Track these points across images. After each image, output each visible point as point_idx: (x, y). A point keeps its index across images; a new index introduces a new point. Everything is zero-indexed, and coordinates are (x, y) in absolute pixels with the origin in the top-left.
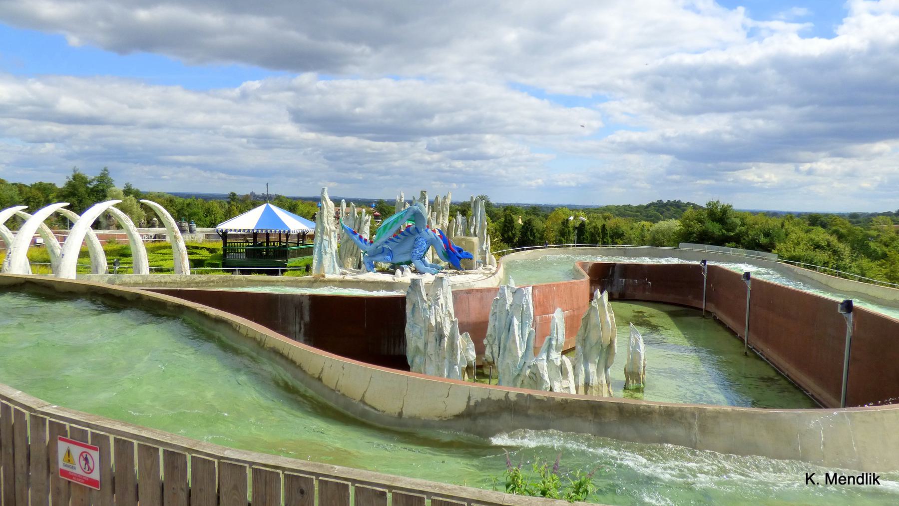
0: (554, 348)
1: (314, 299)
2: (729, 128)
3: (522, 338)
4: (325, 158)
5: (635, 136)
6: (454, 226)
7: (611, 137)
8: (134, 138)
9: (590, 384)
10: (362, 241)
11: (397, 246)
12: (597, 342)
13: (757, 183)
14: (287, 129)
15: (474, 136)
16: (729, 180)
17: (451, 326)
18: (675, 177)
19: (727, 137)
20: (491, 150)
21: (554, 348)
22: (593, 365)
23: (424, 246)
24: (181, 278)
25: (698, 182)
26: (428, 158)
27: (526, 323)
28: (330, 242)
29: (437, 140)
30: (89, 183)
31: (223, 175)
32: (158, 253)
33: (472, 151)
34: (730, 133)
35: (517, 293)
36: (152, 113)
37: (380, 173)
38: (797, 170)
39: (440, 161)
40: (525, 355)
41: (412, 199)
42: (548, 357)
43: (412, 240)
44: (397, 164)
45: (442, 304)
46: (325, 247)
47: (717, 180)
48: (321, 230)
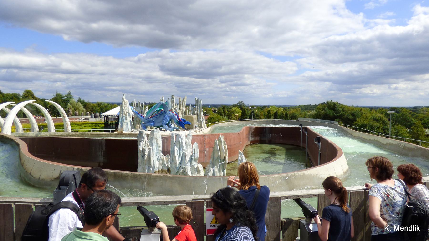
0: (193, 159)
1: (106, 140)
2: (357, 69)
3: (179, 155)
5: (314, 74)
6: (188, 111)
7: (303, 74)
8: (94, 79)
10: (142, 117)
11: (156, 119)
13: (370, 94)
15: (240, 75)
16: (357, 93)
17: (149, 150)
18: (332, 92)
19: (355, 73)
20: (248, 82)
23: (168, 119)
24: (64, 133)
25: (343, 94)
26: (220, 86)
28: (126, 118)
29: (224, 78)
31: (132, 95)
32: (83, 126)
33: (239, 82)
34: (357, 71)
35: (177, 136)
37: (200, 93)
38: (390, 88)
39: (225, 87)
41: (194, 102)
42: (191, 164)
43: (162, 117)
44: (207, 88)
45: (145, 141)
46: (124, 120)
47: (351, 93)
48: (122, 112)
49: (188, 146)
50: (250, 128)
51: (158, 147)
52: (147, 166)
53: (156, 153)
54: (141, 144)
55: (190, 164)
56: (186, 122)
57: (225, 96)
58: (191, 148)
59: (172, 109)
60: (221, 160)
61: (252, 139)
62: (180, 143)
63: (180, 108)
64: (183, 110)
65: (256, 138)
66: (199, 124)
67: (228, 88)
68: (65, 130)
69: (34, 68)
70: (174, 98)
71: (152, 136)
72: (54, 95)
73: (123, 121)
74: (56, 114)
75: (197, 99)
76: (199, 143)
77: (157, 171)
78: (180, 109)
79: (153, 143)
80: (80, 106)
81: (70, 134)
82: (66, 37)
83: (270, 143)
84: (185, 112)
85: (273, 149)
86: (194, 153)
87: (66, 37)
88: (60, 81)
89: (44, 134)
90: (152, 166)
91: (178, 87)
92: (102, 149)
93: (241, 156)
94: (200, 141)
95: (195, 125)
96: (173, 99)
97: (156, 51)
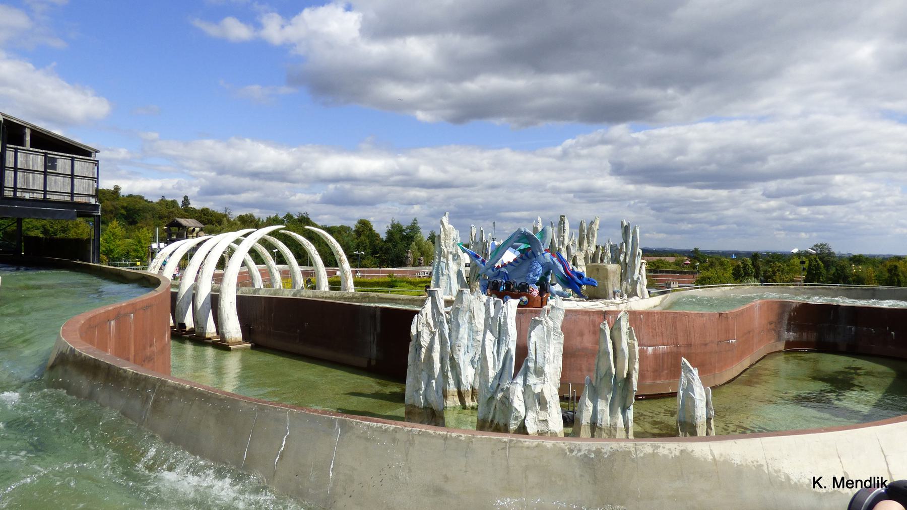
0: (532, 370)
1: (384, 309)
3: (498, 356)
4: (653, 209)
6: (600, 253)
9: (598, 425)
11: (514, 269)
12: (606, 372)
14: (609, 183)
17: (430, 337)
21: (532, 370)
22: (604, 401)
23: (539, 270)
26: (764, 205)
27: (503, 340)
28: (447, 264)
30: (404, 231)
36: (488, 176)
37: (713, 223)
39: (780, 208)
40: (500, 376)
42: (525, 380)
43: (528, 263)
44: (730, 212)
46: (442, 269)
48: (439, 252)
49: (552, 337)
50: (783, 305)
51: (473, 332)
52: (424, 375)
53: (467, 346)
54: (416, 321)
55: (522, 382)
56: (584, 280)
57: (782, 232)
58: (560, 343)
59: (561, 247)
60: (618, 380)
61: (792, 336)
62: (500, 323)
63: (582, 247)
64: (588, 252)
65: (805, 335)
66: (629, 287)
67: (788, 213)
68: (342, 287)
69: (372, 180)
70: (567, 222)
71: (457, 305)
72: (388, 227)
73: (440, 271)
74: (389, 262)
75: (625, 224)
76: (589, 332)
77: (468, 390)
78: (581, 250)
79: (460, 322)
80: (431, 248)
81: (345, 296)
82: (421, 115)
83: (852, 351)
84: (595, 256)
85: (853, 371)
86: (534, 354)
87: (421, 115)
88: (417, 203)
89: (308, 294)
90: (436, 377)
91: (659, 210)
92: (375, 329)
93: (687, 376)
94: (591, 326)
95: (613, 288)
96: (564, 223)
97: (598, 132)
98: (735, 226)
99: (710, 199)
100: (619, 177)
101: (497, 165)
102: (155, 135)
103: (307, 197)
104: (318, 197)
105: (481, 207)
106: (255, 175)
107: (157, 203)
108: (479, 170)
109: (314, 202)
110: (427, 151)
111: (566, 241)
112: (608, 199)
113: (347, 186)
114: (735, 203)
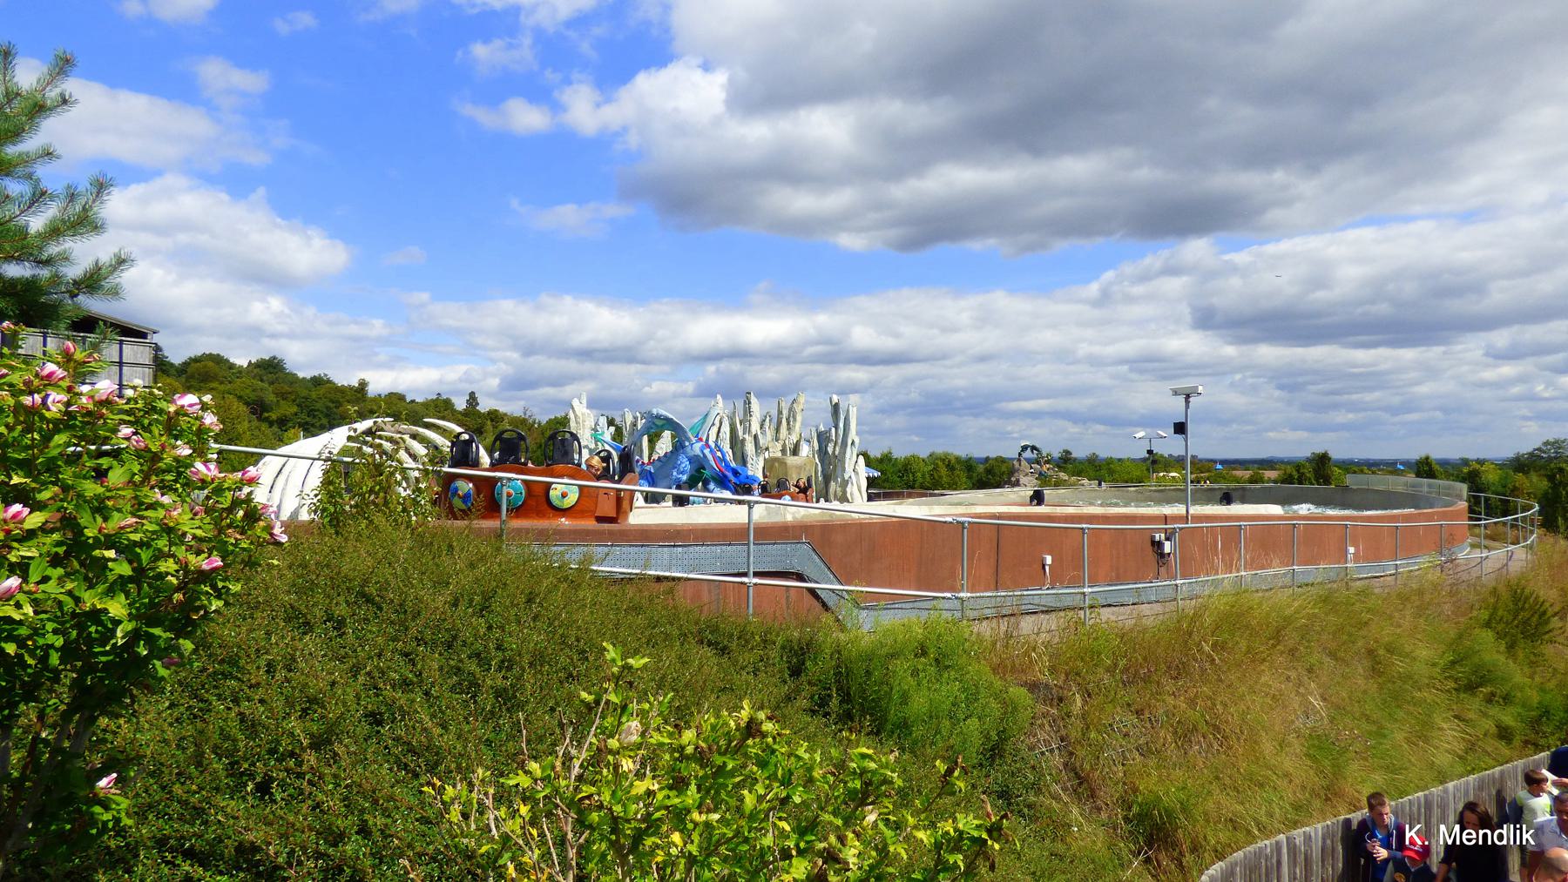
4: (1281, 387)
14: (1189, 344)
37: (1394, 411)
44: (1424, 389)
59: (746, 436)
91: (1292, 388)
98: (1438, 414)
99: (1383, 367)
100: (1209, 333)
101: (984, 320)
102: (424, 296)
103: (671, 387)
104: (690, 387)
105: (962, 394)
106: (586, 354)
107: (422, 404)
108: (954, 329)
109: (684, 395)
110: (862, 301)
111: (755, 427)
112: (1193, 372)
113: (734, 367)
114: (1431, 372)
